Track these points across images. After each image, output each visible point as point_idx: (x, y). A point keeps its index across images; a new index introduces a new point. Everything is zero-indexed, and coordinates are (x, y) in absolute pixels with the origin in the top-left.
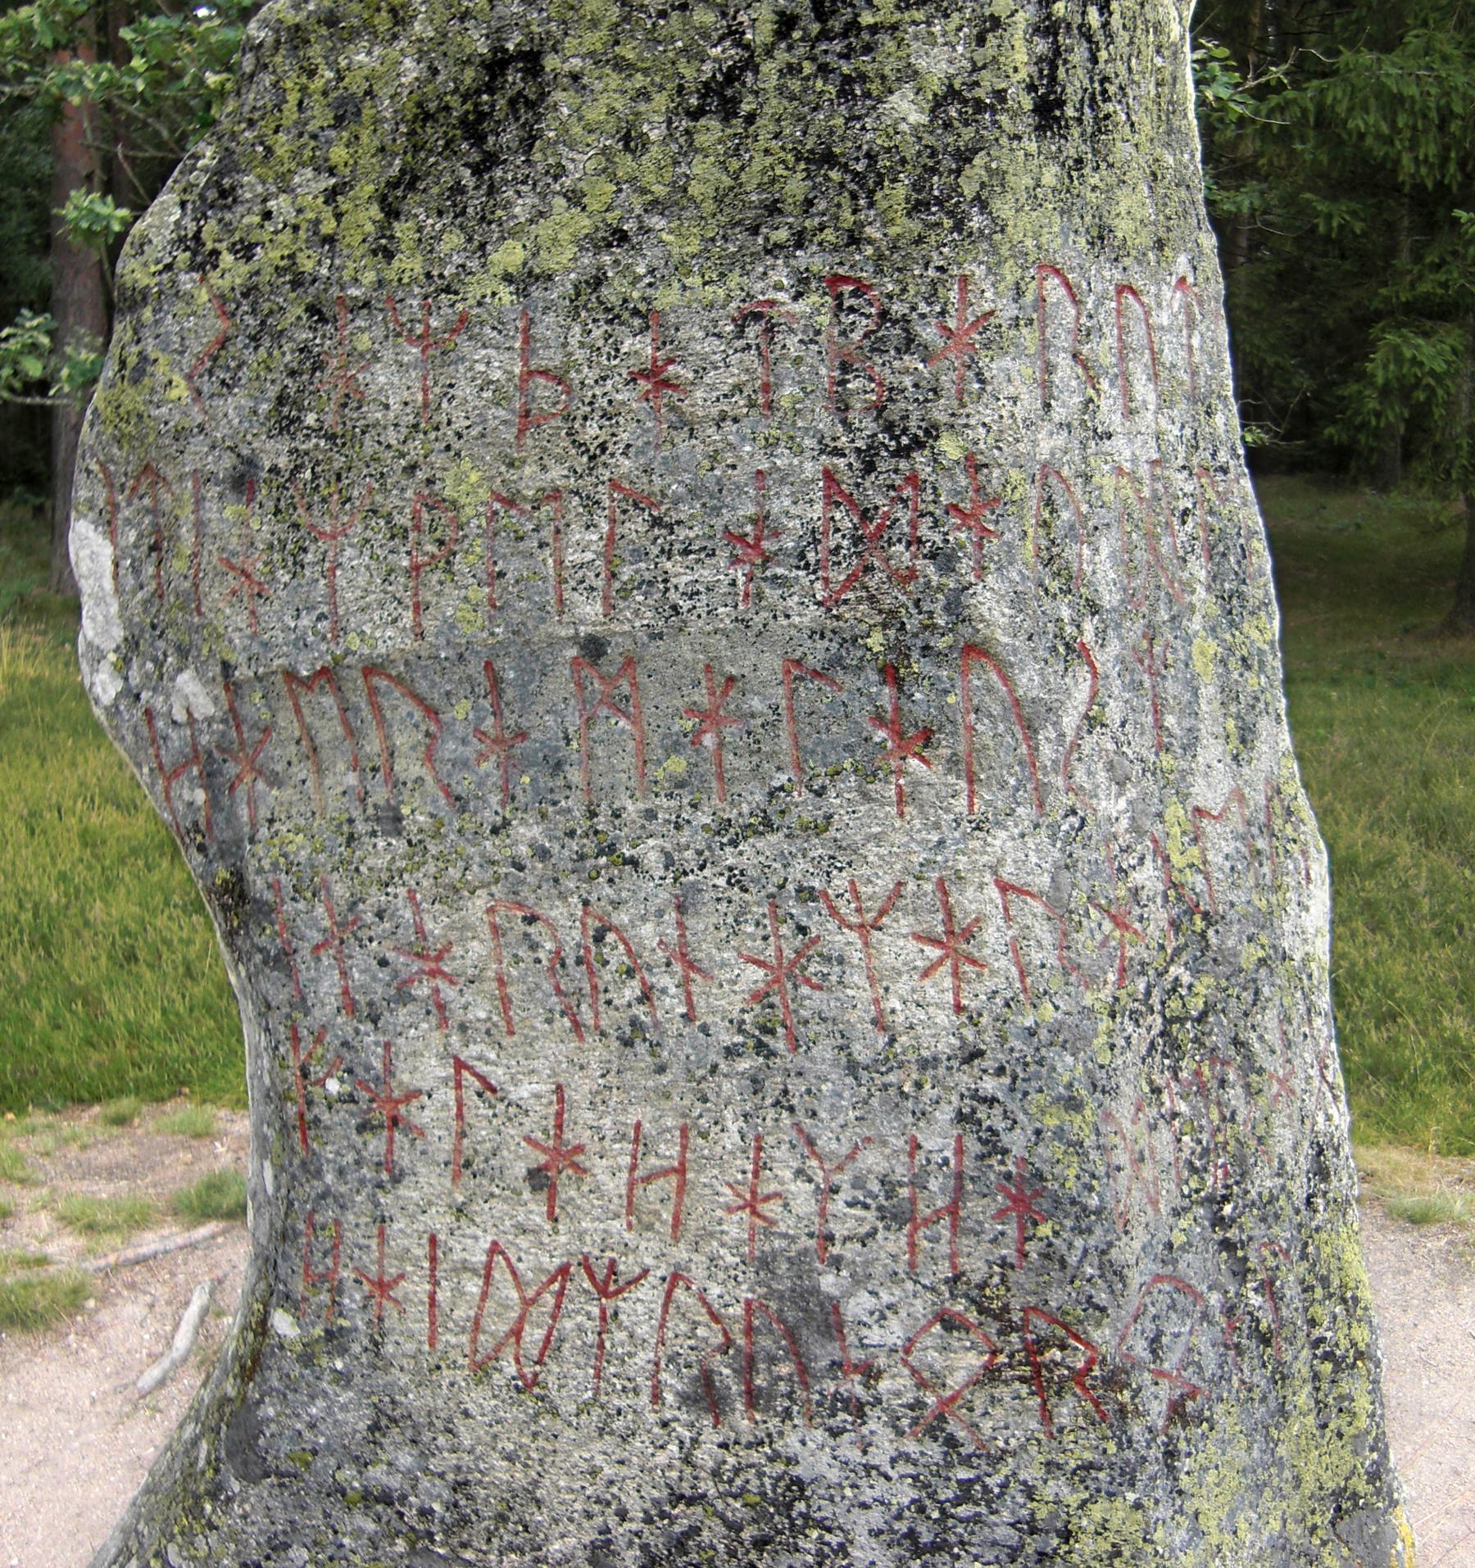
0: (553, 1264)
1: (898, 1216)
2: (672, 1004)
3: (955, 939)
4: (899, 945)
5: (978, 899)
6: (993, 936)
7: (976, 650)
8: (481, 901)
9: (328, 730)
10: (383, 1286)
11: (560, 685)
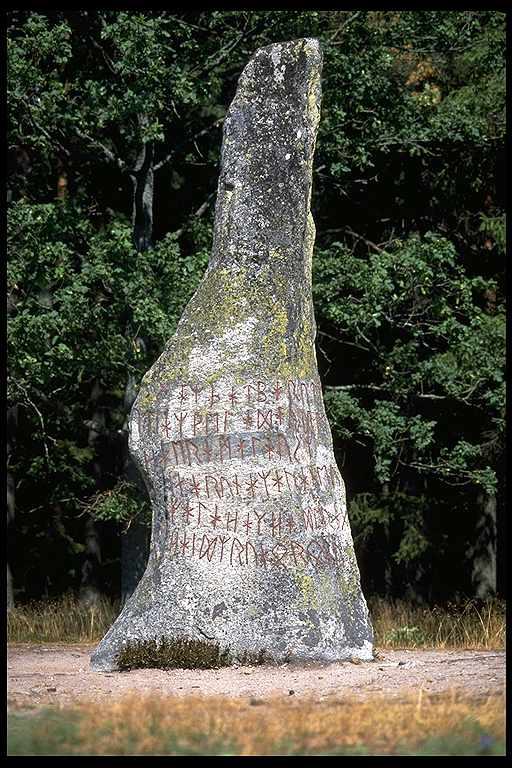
0: (214, 537)
1: (272, 525)
2: (235, 491)
3: (278, 481)
4: (269, 481)
5: (280, 474)
6: (284, 480)
7: (280, 435)
8: (204, 476)
9: (179, 451)
10: (185, 545)
11: (217, 443)
